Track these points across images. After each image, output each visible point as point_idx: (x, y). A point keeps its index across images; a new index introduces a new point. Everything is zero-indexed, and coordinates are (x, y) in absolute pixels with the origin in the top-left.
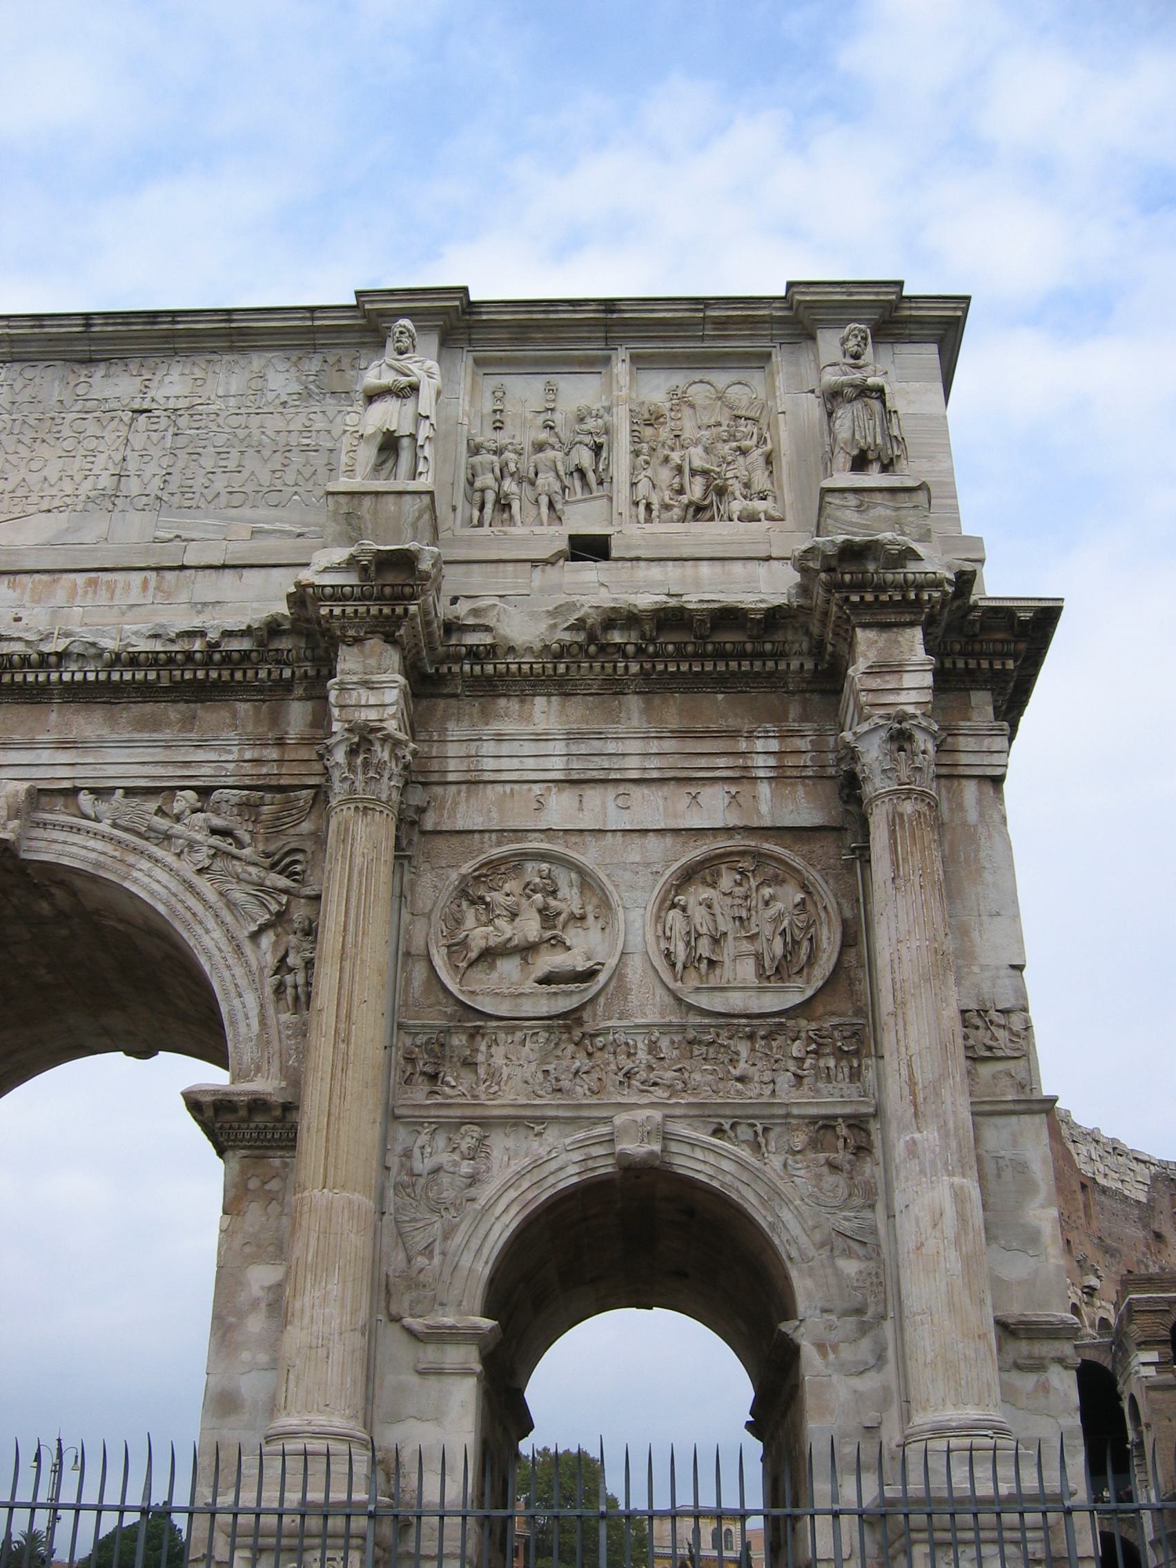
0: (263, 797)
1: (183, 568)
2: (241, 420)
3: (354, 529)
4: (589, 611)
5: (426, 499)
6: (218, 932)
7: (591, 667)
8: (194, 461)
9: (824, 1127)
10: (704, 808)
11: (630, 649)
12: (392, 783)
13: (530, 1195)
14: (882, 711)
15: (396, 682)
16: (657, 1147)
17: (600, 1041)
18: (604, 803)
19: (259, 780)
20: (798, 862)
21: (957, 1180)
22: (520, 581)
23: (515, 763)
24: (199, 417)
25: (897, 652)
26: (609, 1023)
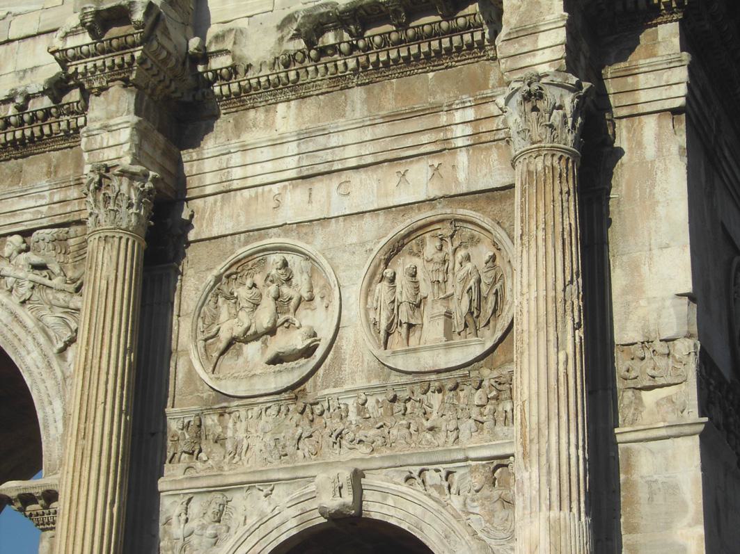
0: (68, 232)
1: (8, 41)
6: (36, 352)
9: (498, 466)
10: (411, 184)
11: (344, 47)
12: (131, 211)
17: (318, 409)
18: (329, 193)
19: (65, 217)
20: (486, 222)
25: (536, 13)
26: (326, 392)
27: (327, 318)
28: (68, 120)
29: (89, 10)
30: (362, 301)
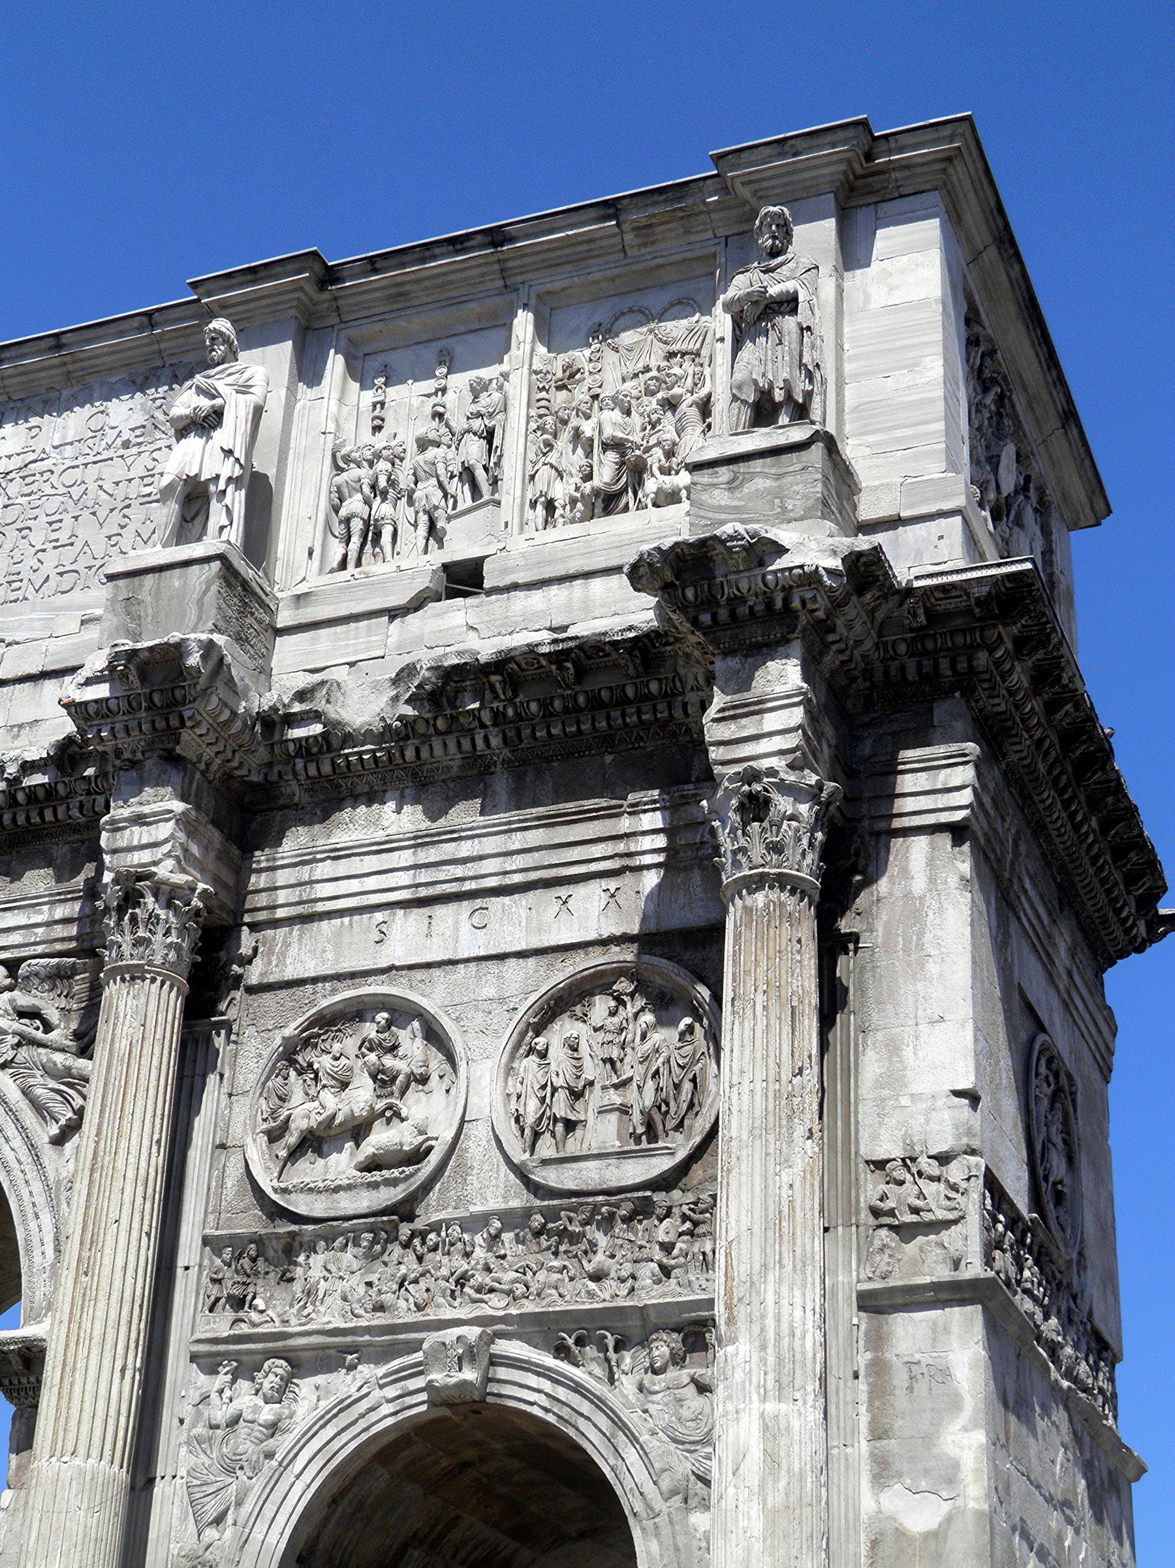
2: (77, 474)
3: (133, 619)
4: (427, 674)
5: (216, 565)
7: (445, 744)
8: (23, 538)
12: (169, 940)
13: (336, 1444)
14: (732, 770)
15: (171, 811)
16: (470, 1374)
18: (456, 923)
21: (770, 1407)
22: (373, 639)
23: (354, 885)
24: (32, 478)
26: (442, 1216)
27: (448, 1104)
28: (81, 802)
29: (123, 648)
30: (501, 1083)
